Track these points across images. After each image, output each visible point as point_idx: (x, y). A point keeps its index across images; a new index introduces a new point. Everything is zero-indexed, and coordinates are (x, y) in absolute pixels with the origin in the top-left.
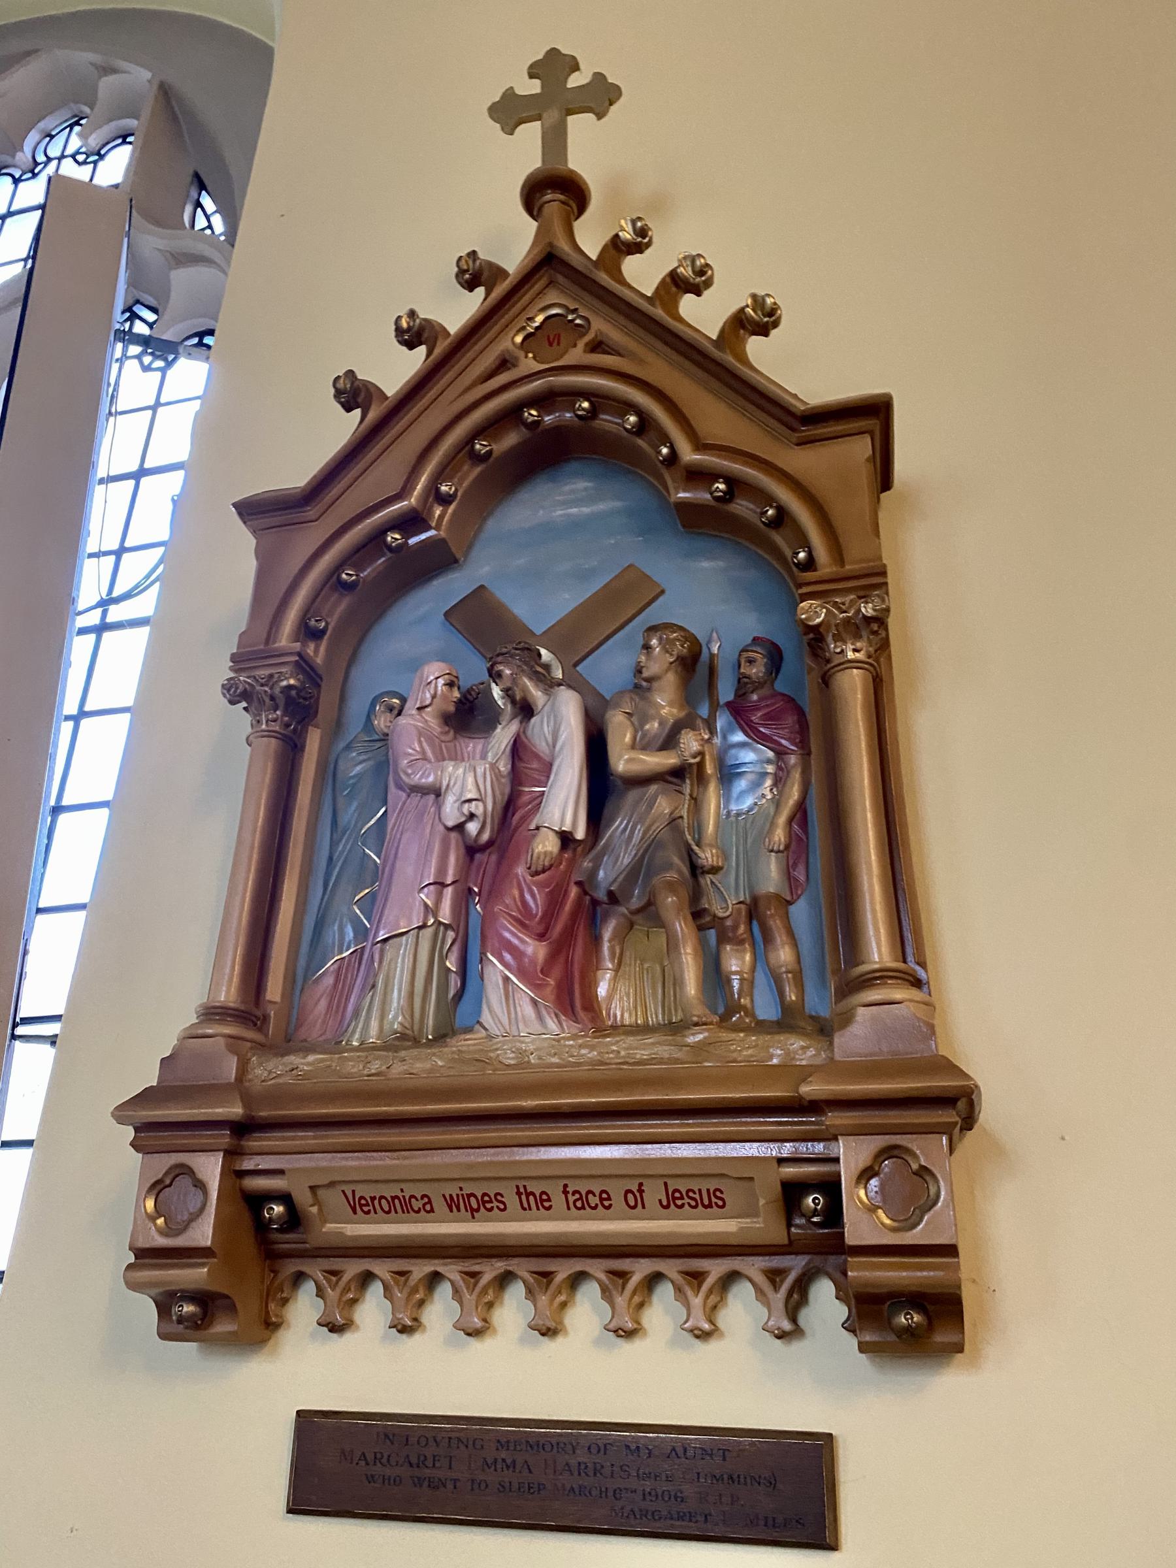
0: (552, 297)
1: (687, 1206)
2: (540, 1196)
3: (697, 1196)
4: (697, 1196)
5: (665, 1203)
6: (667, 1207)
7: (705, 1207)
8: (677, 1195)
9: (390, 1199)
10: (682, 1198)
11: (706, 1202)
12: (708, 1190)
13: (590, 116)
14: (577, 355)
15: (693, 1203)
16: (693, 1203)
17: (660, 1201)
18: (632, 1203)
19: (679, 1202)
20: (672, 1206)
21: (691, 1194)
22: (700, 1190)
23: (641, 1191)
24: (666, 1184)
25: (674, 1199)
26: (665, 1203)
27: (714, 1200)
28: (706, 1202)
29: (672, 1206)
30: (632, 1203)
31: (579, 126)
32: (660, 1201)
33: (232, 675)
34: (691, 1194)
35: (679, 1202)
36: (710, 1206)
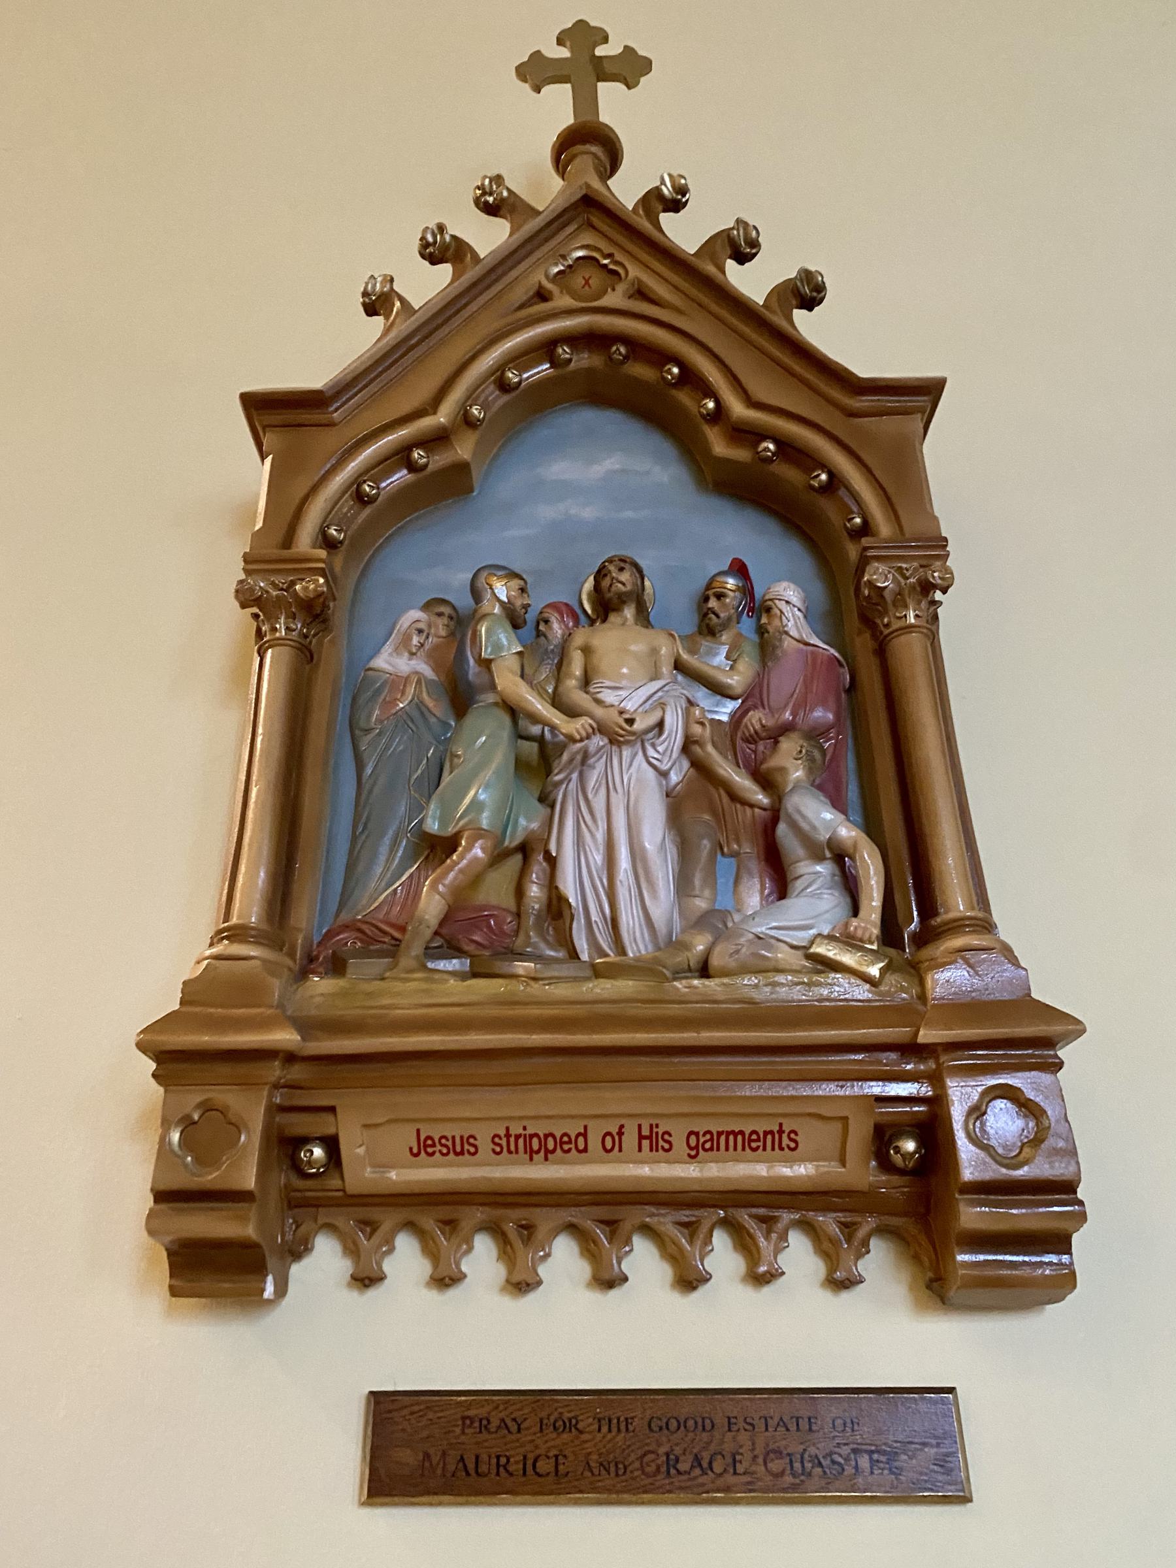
0: (588, 238)
1: (438, 1154)
2: (468, 1139)
3: (450, 1144)
4: (450, 1144)
5: (415, 1150)
6: (417, 1155)
7: (457, 1154)
8: (429, 1142)
9: (542, 1136)
10: (433, 1145)
11: (458, 1149)
12: (462, 1137)
13: (620, 86)
14: (615, 298)
15: (445, 1151)
16: (445, 1151)
17: (411, 1149)
18: (609, 1145)
19: (430, 1150)
20: (559, 1150)
21: (443, 1141)
22: (453, 1137)
23: (620, 1134)
24: (418, 1131)
25: (426, 1146)
26: (415, 1150)
27: (466, 1147)
28: (458, 1149)
29: (559, 1150)
30: (609, 1145)
31: (605, 90)
32: (411, 1149)
33: (243, 577)
34: (443, 1141)
35: (430, 1150)
36: (462, 1153)
